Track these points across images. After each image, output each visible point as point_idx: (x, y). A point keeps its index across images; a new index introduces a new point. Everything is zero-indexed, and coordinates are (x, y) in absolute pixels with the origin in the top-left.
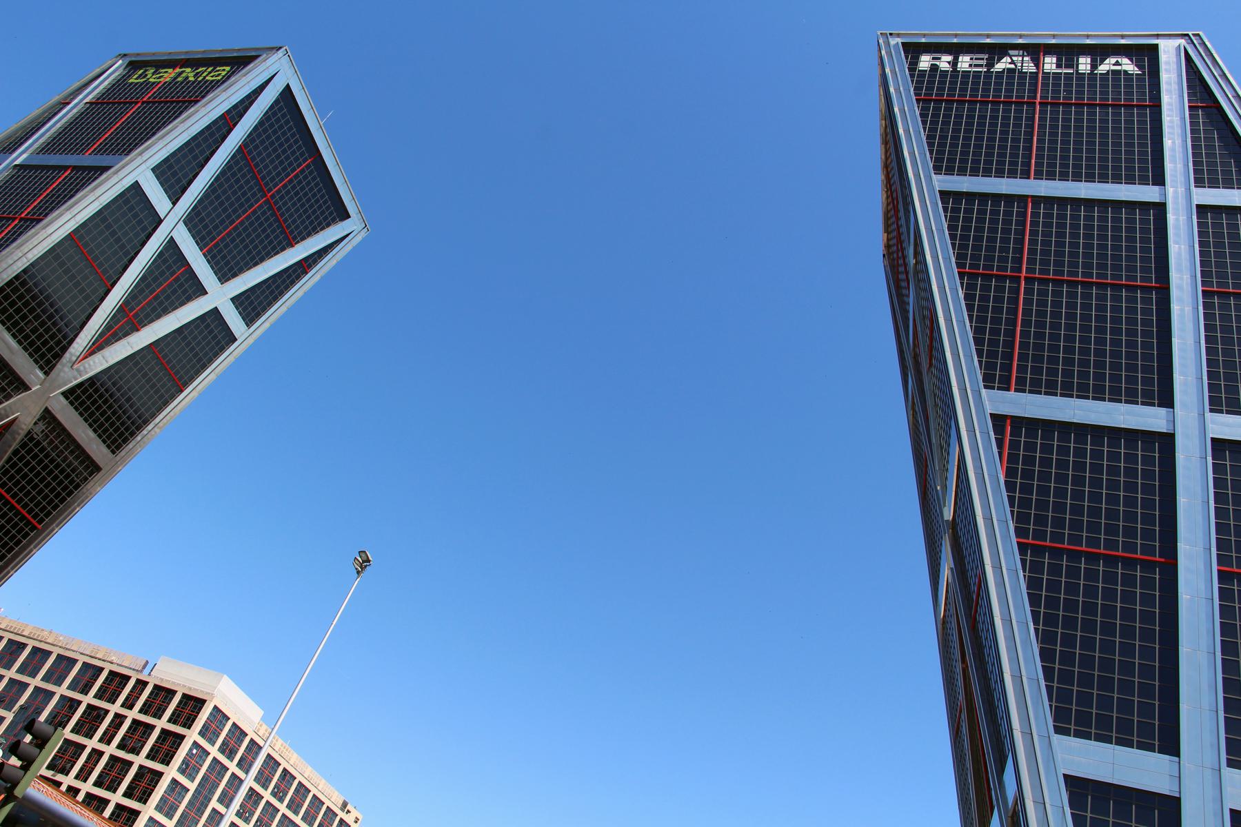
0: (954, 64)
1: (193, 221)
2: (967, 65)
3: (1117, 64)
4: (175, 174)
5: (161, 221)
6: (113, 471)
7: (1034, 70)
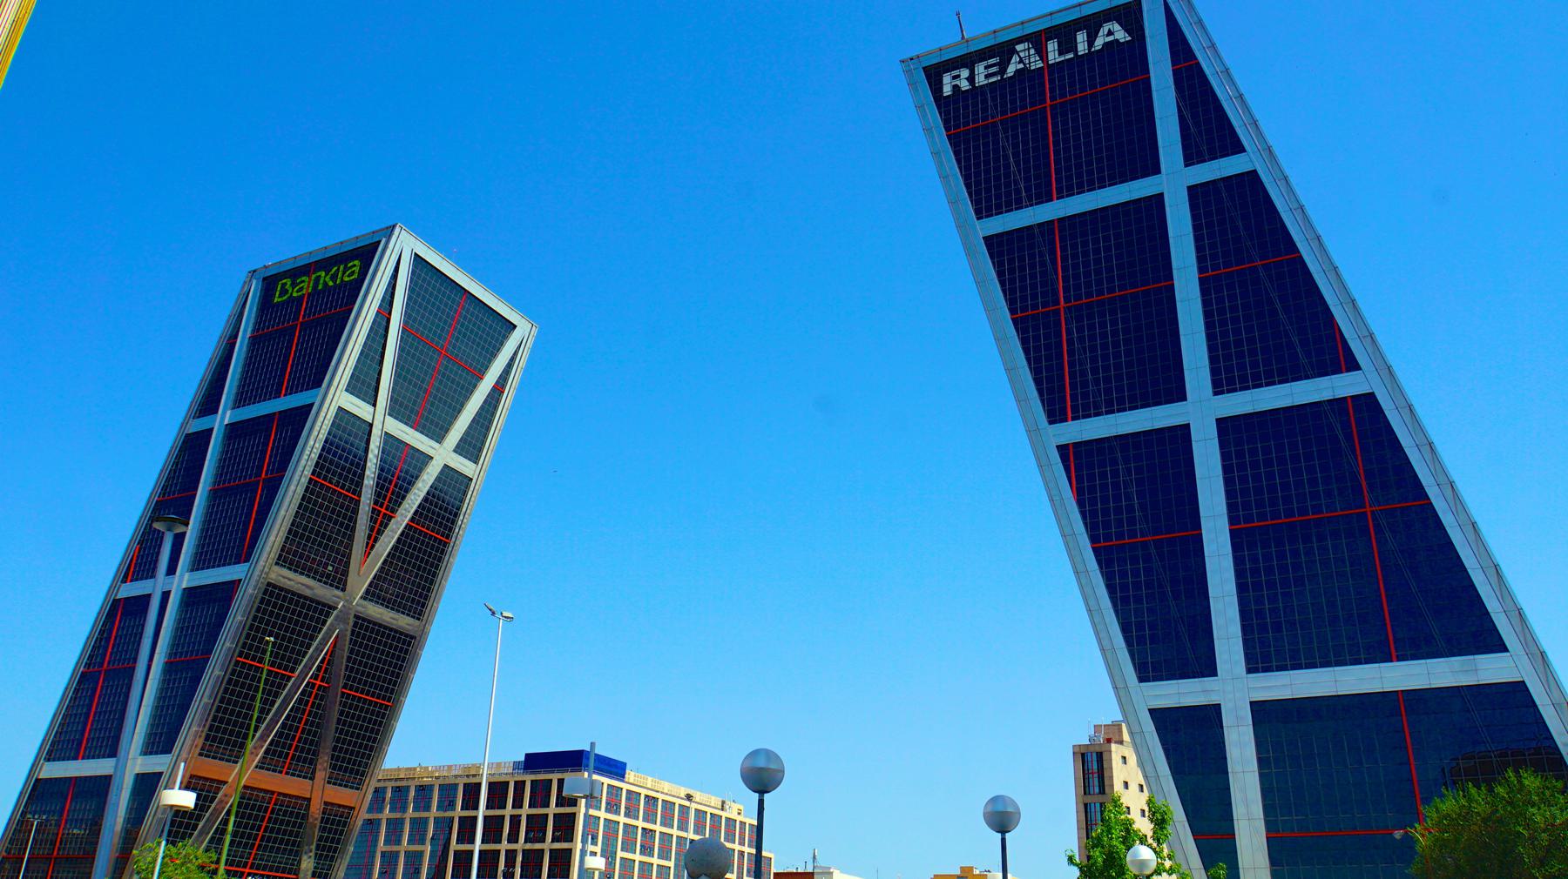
0: (971, 79)
1: (395, 410)
2: (982, 77)
4: (364, 385)
5: (371, 425)
6: (424, 633)
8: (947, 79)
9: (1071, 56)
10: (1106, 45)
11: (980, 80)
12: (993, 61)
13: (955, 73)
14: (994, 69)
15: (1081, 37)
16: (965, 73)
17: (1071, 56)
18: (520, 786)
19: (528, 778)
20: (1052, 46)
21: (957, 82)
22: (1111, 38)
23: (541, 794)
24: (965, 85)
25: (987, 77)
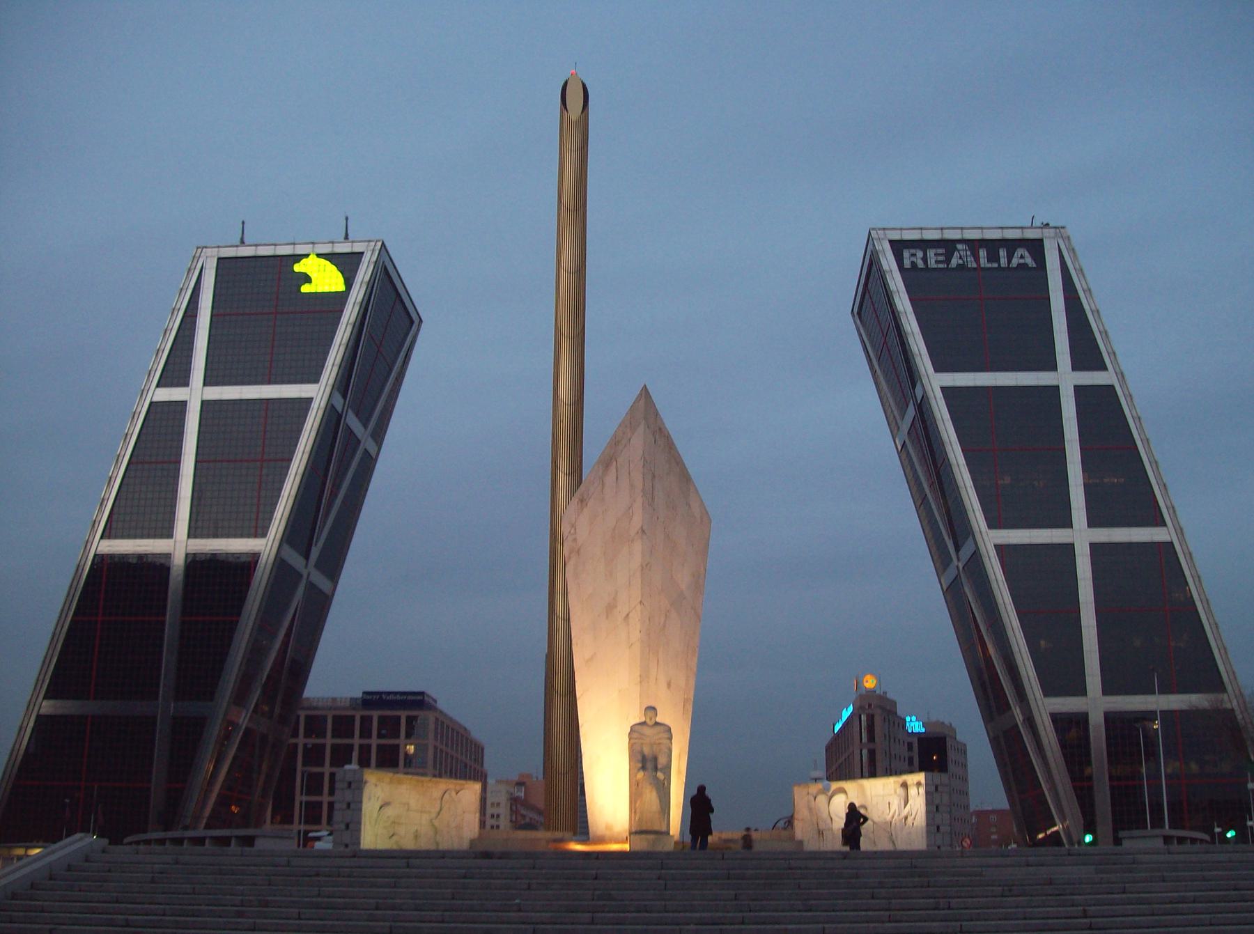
0: (925, 259)
3: (1022, 257)
7: (975, 265)
8: (906, 254)
9: (996, 265)
10: (1019, 265)
11: (932, 263)
12: (941, 251)
13: (913, 251)
14: (941, 258)
15: (1003, 253)
16: (920, 254)
17: (996, 265)
18: (366, 721)
19: (376, 714)
20: (983, 253)
21: (913, 259)
22: (1022, 261)
23: (390, 727)
24: (920, 264)
25: (937, 262)
